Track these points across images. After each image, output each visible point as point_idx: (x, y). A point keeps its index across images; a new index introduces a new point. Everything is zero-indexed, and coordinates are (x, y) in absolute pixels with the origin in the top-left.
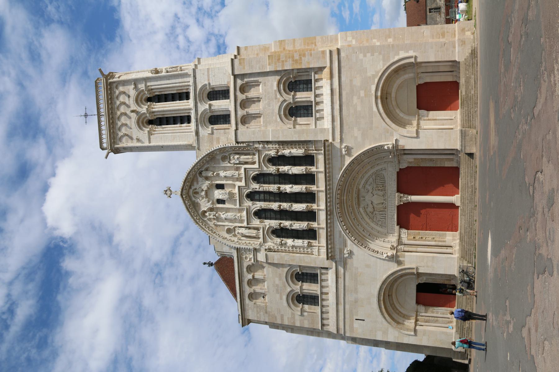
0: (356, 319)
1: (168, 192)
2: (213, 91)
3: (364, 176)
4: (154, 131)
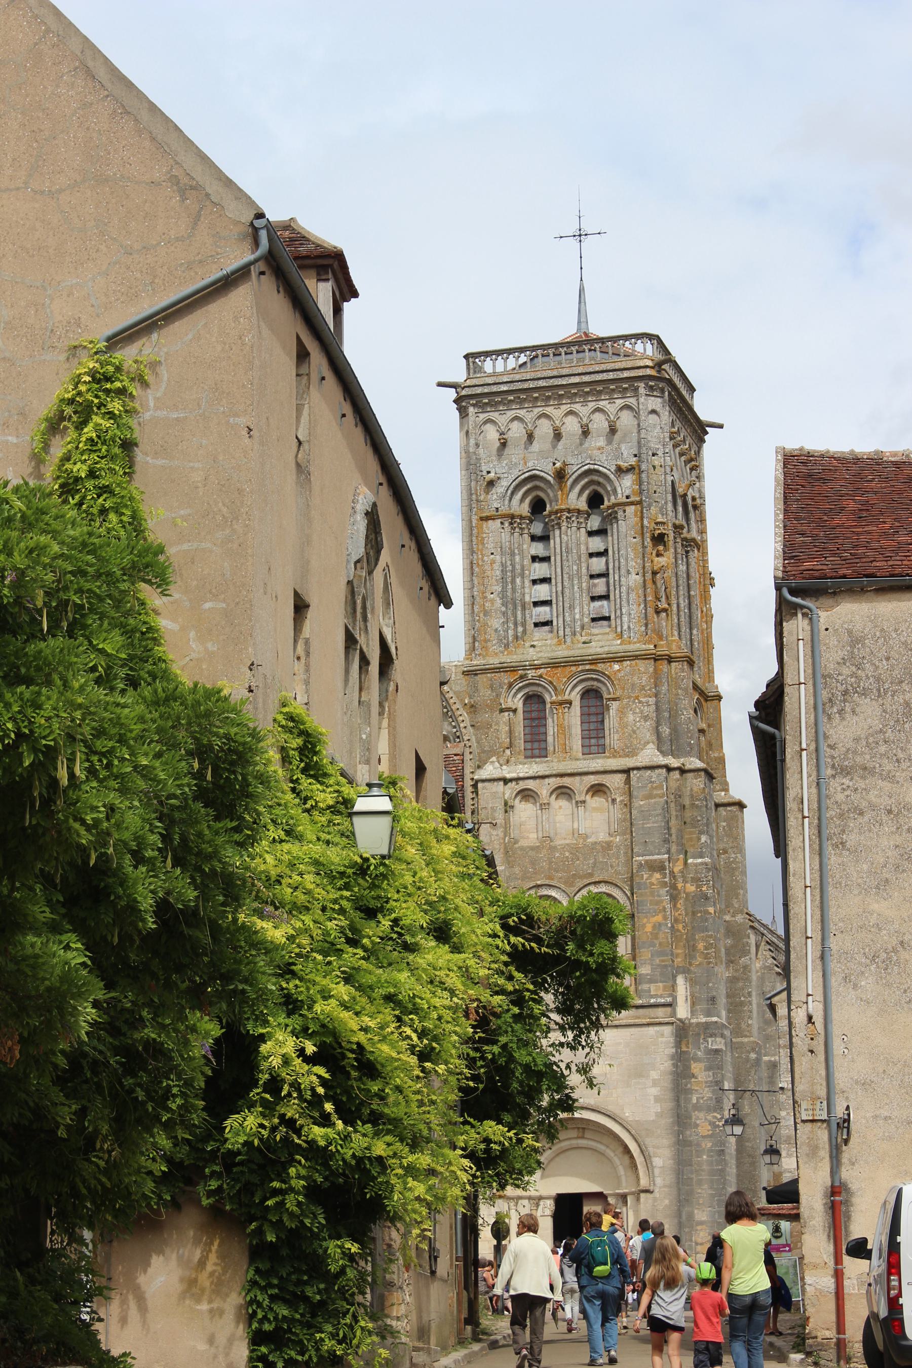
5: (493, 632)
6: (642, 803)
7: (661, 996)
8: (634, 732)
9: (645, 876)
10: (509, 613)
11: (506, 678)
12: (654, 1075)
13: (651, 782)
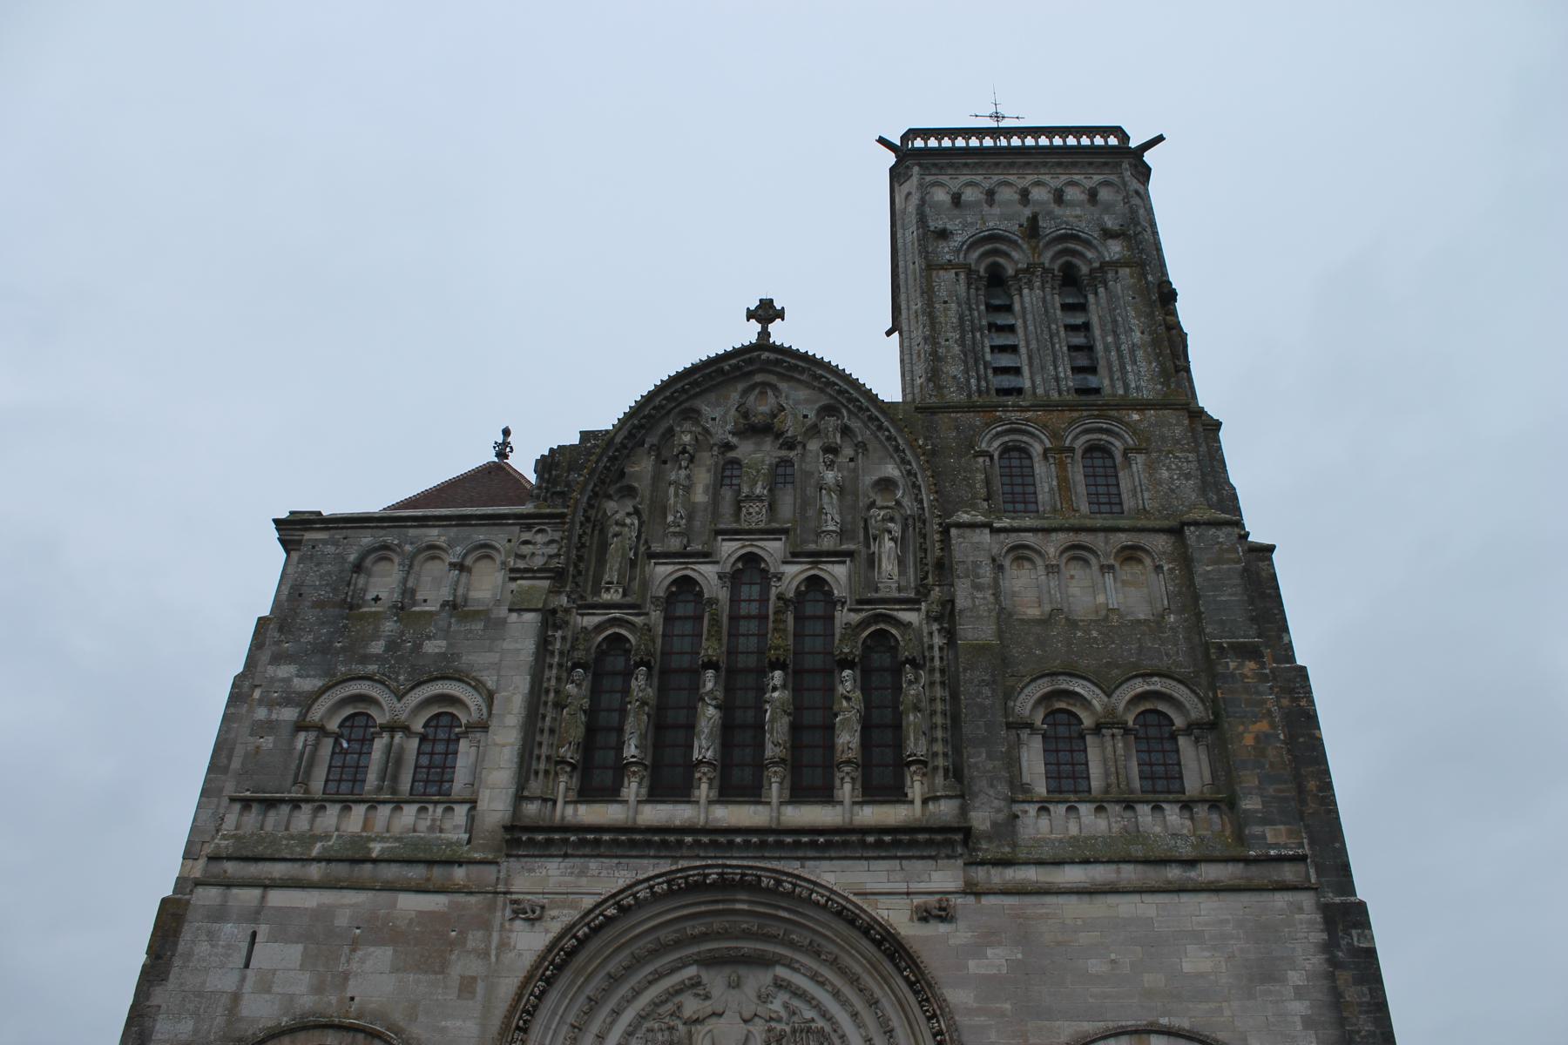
0: (254, 935)
1: (766, 312)
2: (1115, 467)
3: (822, 984)
4: (969, 285)
6: (1209, 568)
7: (1285, 847)
8: (1173, 491)
9: (1232, 665)
10: (971, 362)
11: (977, 420)
12: (1295, 978)
13: (1218, 543)
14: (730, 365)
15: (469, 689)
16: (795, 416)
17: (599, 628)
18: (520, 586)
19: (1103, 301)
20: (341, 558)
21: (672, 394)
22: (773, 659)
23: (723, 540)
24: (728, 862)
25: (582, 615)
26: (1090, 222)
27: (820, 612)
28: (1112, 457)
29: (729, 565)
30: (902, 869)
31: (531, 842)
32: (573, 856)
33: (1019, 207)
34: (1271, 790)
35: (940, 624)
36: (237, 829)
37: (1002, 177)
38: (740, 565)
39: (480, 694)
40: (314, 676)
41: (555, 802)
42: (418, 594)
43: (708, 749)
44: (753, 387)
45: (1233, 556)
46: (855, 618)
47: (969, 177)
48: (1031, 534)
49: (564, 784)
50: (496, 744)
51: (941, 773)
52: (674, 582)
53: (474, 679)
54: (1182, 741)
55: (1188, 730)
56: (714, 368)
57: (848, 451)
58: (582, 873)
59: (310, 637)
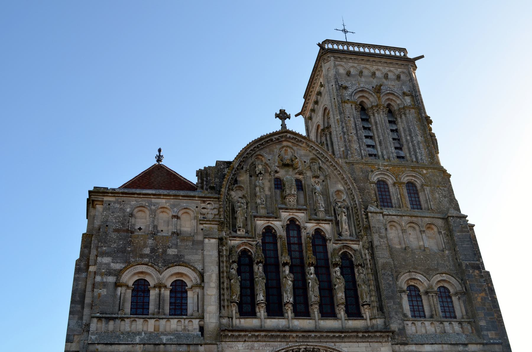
5: (354, 150)
6: (459, 234)
7: (495, 339)
8: (440, 202)
9: (471, 271)
13: (461, 224)
14: (275, 138)
15: (190, 270)
16: (301, 162)
17: (239, 246)
18: (206, 227)
19: (404, 122)
20: (122, 210)
21: (254, 148)
22: (311, 262)
23: (282, 212)
24: (308, 344)
25: (231, 240)
26: (398, 88)
27: (321, 243)
28: (416, 187)
29: (285, 222)
30: (370, 346)
31: (232, 336)
32: (247, 341)
33: (372, 79)
34: (488, 318)
35: (368, 251)
36: (96, 330)
37: (364, 65)
38: (288, 222)
39: (196, 273)
40: (120, 263)
41: (232, 318)
42: (158, 227)
43: (291, 298)
44: (283, 147)
45: (466, 230)
46: (336, 246)
47: (352, 64)
48: (396, 217)
49: (234, 309)
50: (208, 295)
51: (376, 308)
52: (265, 228)
53: (192, 266)
54: (454, 299)
55: (456, 294)
56: (269, 139)
57: (322, 177)
58: (252, 348)
59: (115, 245)
